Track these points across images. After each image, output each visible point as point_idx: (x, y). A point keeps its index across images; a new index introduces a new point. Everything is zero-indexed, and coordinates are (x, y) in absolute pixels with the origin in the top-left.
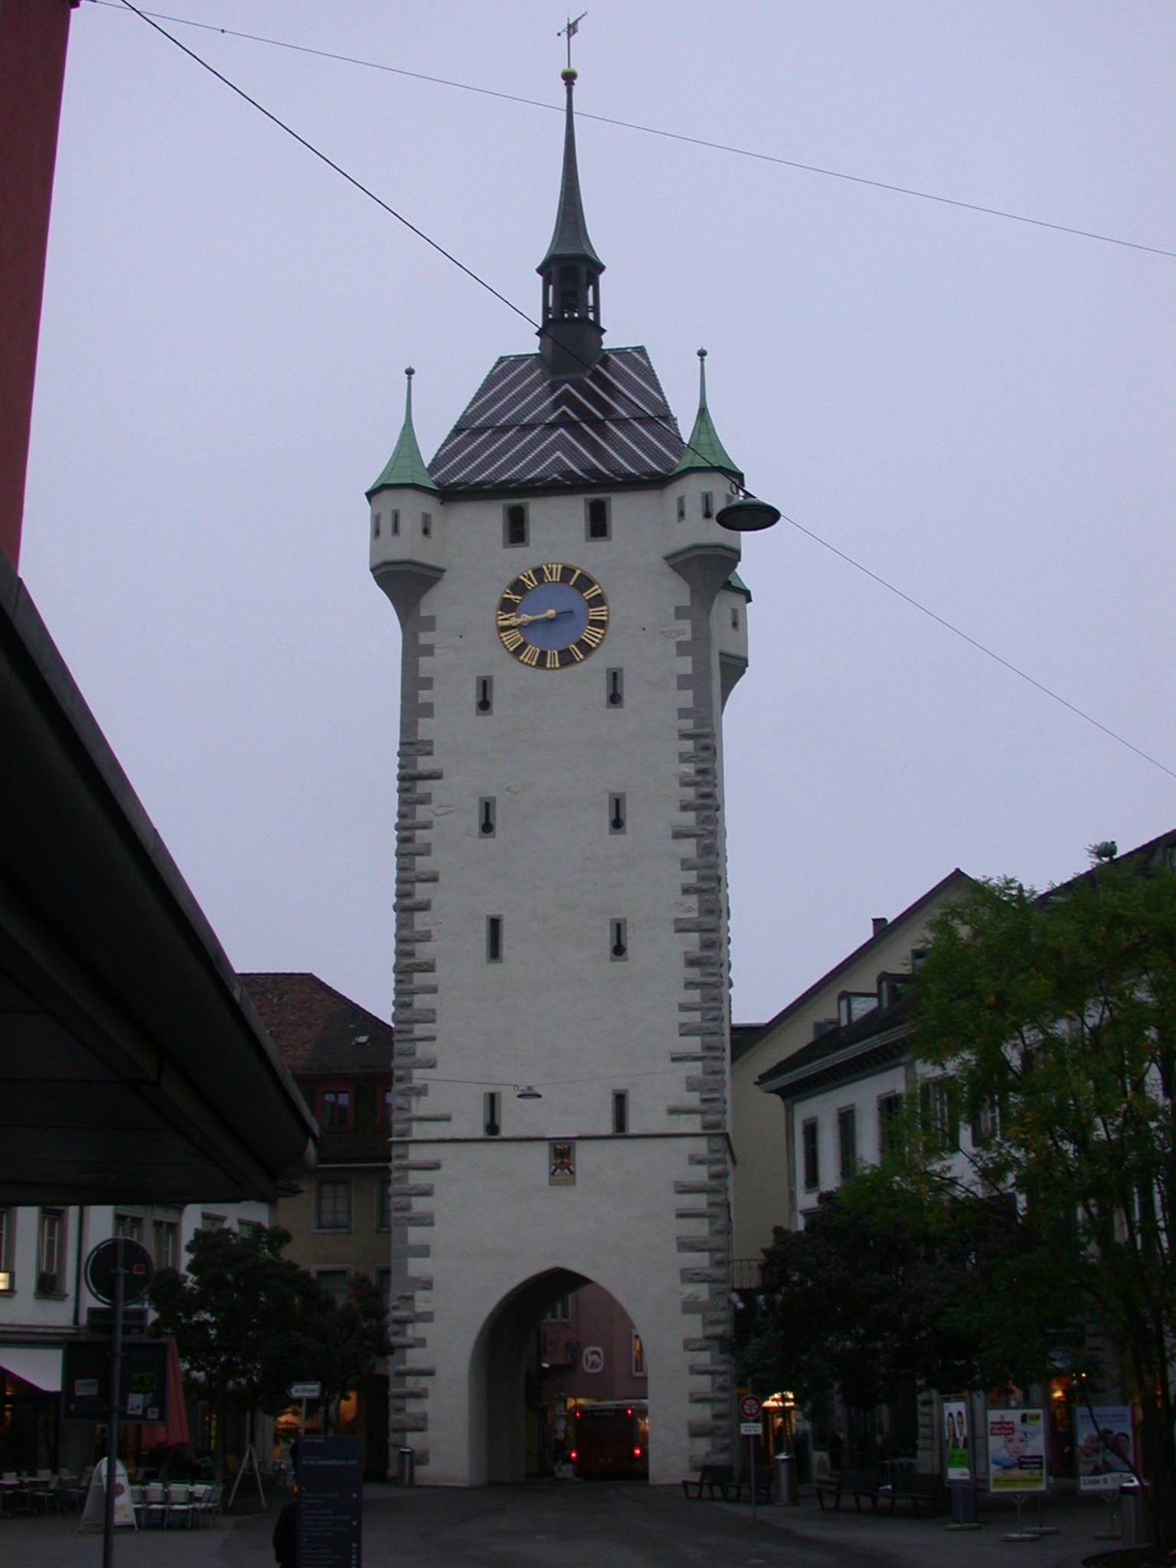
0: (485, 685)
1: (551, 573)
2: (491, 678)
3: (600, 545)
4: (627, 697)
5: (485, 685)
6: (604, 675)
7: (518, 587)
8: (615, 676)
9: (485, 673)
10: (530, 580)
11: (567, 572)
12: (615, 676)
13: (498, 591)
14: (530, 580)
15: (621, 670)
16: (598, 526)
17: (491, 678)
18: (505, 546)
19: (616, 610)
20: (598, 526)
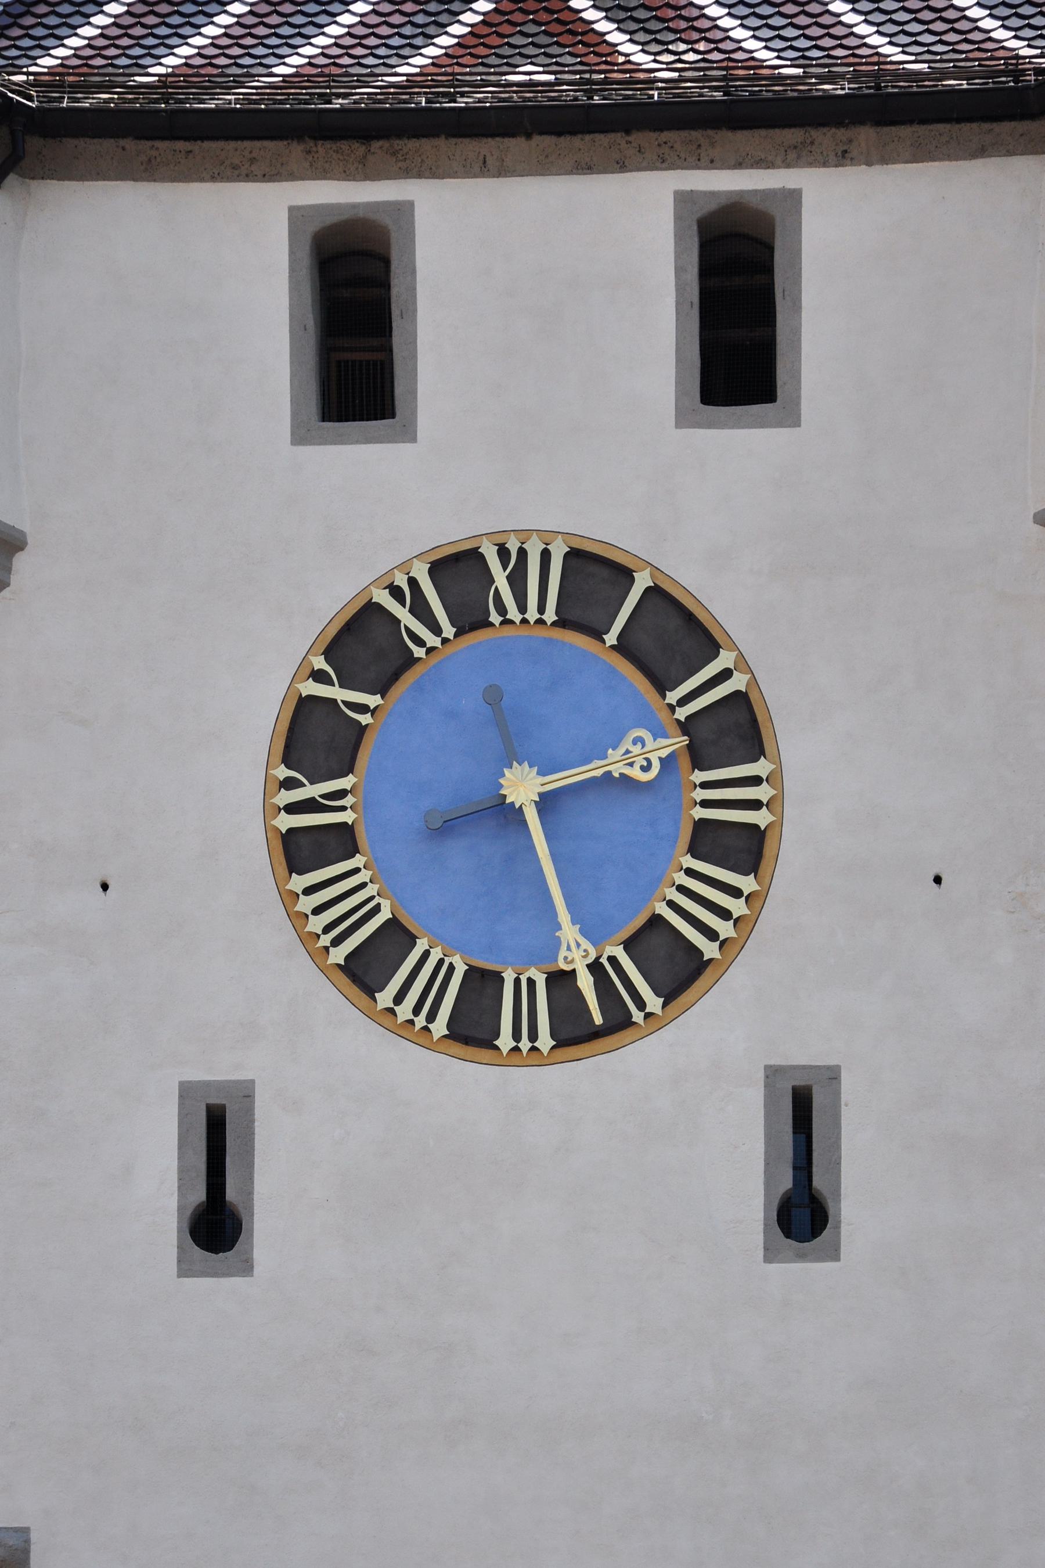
0: (217, 1133)
1: (517, 580)
2: (246, 1092)
3: (741, 445)
4: (854, 1210)
5: (217, 1133)
6: (755, 1097)
7: (365, 646)
8: (802, 1112)
9: (219, 1068)
10: (421, 610)
11: (592, 577)
12: (802, 1112)
13: (272, 665)
14: (421, 610)
15: (833, 1075)
16: (737, 340)
17: (246, 1092)
18: (300, 437)
19: (817, 777)
20: (737, 340)
